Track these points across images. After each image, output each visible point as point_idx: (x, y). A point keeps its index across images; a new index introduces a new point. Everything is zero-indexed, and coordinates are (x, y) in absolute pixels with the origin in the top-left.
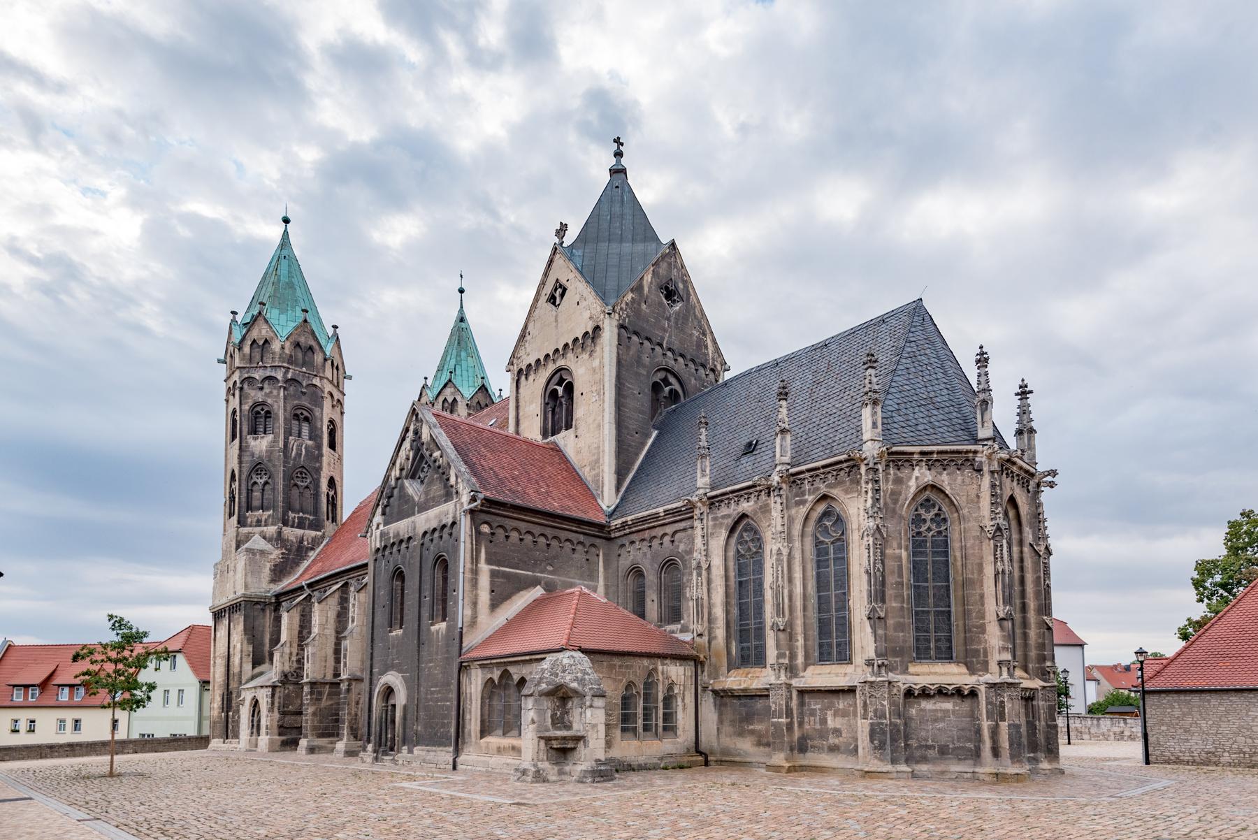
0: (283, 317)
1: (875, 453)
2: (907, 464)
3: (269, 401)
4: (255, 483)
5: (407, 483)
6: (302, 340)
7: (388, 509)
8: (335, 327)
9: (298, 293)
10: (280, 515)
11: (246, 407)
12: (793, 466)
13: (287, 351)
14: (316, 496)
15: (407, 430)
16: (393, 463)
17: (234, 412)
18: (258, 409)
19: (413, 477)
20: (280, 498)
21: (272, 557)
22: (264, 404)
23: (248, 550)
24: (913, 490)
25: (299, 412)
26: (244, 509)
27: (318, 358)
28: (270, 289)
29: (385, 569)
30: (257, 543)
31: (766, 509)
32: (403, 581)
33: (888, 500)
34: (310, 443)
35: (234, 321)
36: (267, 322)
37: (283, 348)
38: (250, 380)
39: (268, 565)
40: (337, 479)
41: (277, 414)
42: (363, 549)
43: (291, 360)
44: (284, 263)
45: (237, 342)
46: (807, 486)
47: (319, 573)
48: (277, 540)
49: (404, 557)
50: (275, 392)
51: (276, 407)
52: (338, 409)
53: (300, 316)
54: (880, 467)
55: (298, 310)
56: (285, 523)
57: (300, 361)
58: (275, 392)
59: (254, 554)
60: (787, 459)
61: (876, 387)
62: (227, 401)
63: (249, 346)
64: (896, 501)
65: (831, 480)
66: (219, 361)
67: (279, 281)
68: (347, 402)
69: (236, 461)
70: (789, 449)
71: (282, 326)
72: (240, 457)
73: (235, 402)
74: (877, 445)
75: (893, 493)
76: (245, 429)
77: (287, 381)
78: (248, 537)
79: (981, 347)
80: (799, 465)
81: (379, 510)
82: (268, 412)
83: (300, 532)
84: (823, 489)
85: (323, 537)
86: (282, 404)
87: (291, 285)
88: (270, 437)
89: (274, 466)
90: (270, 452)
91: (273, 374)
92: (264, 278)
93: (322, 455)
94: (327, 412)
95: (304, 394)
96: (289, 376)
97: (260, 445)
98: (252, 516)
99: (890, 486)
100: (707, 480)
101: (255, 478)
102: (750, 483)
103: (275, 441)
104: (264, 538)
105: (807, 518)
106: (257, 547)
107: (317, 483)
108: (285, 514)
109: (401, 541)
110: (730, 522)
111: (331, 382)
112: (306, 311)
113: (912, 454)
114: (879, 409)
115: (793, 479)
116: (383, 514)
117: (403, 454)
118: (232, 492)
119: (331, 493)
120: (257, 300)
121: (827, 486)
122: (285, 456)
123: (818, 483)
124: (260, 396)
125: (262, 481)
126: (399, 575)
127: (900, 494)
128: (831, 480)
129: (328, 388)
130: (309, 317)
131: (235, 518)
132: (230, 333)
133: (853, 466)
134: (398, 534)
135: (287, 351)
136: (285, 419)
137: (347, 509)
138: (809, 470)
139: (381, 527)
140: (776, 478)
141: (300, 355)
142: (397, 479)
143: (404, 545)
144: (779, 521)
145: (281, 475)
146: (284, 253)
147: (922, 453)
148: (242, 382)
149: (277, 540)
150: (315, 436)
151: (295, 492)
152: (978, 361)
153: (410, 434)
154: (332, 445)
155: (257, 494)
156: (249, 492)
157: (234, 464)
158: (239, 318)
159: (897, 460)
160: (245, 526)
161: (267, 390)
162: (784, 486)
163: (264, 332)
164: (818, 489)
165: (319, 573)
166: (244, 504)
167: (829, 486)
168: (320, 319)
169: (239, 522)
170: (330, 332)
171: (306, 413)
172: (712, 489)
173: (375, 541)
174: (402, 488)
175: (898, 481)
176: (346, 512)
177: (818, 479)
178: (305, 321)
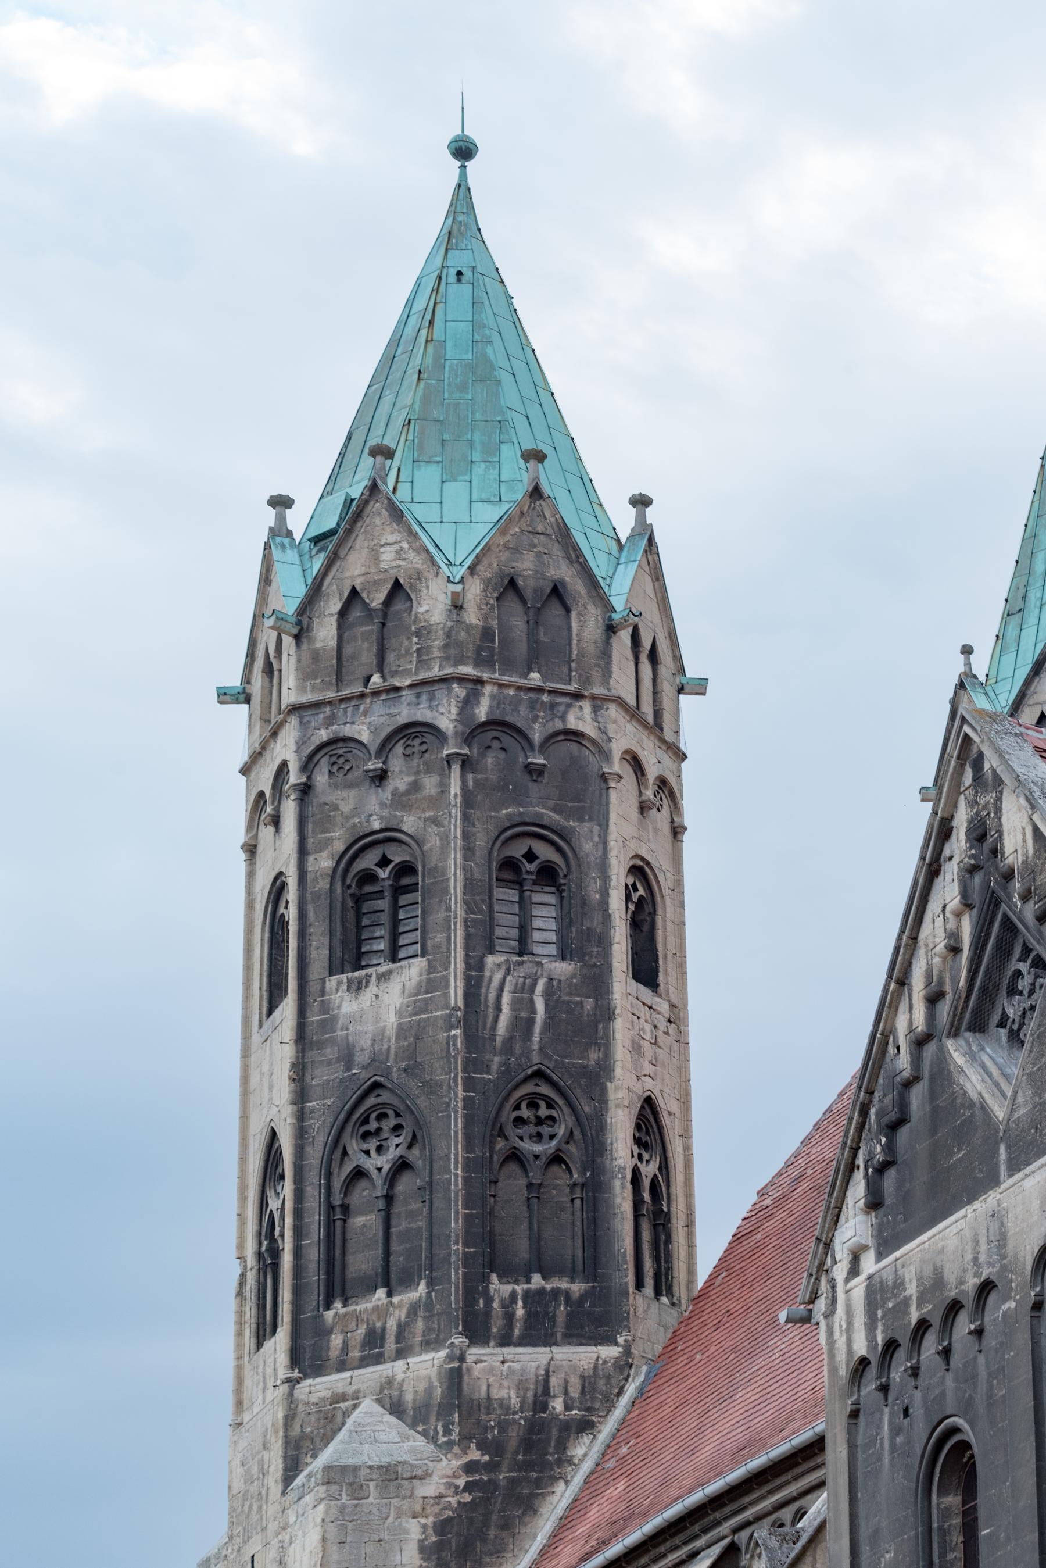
0: (456, 490)
3: (410, 823)
4: (359, 1174)
5: (956, 1052)
6: (525, 566)
7: (890, 1177)
8: (641, 502)
9: (510, 395)
10: (455, 1297)
11: (323, 862)
13: (472, 616)
14: (593, 1190)
15: (941, 831)
16: (899, 977)
17: (278, 888)
18: (368, 861)
19: (978, 1026)
20: (456, 1225)
21: (429, 1489)
22: (390, 836)
23: (334, 1475)
25: (517, 851)
26: (313, 1298)
27: (585, 626)
28: (410, 396)
29: (896, 1445)
30: (373, 1437)
32: (969, 1489)
34: (563, 969)
35: (279, 532)
36: (397, 514)
37: (457, 606)
38: (336, 750)
39: (414, 1530)
40: (667, 1104)
41: (438, 873)
42: (789, 1384)
43: (488, 649)
44: (458, 295)
45: (290, 608)
47: (617, 1526)
48: (445, 1410)
49: (969, 1377)
50: (430, 784)
51: (433, 842)
52: (661, 818)
53: (516, 476)
55: (510, 455)
56: (476, 1330)
57: (521, 649)
58: (430, 784)
59: (357, 1491)
62: (251, 850)
63: (337, 627)
66: (225, 696)
67: (440, 360)
68: (694, 784)
69: (283, 1090)
71: (456, 521)
72: (300, 1071)
73: (281, 851)
76: (319, 954)
77: (475, 732)
78: (331, 1418)
81: (858, 1190)
82: (407, 869)
83: (531, 1359)
85: (624, 1365)
86: (455, 829)
87: (481, 372)
88: (413, 971)
89: (431, 1088)
90: (413, 1033)
91: (423, 714)
92: (389, 359)
93: (607, 1014)
94: (623, 834)
95: (534, 772)
96: (482, 712)
97: (378, 1007)
98: (345, 1321)
101: (358, 1154)
103: (433, 984)
104: (396, 1409)
106: (369, 1455)
107: (592, 1136)
108: (474, 1288)
109: (954, 1307)
111: (634, 713)
112: (539, 457)
116: (874, 1203)
117: (934, 933)
118: (268, 1231)
119: (649, 1170)
120: (369, 445)
122: (472, 1039)
124: (371, 809)
125: (385, 1161)
126: (951, 1462)
129: (625, 736)
130: (550, 479)
131: (280, 1342)
132: (266, 579)
134: (939, 1281)
135: (472, 616)
136: (469, 885)
137: (711, 1226)
139: (869, 1264)
141: (518, 624)
142: (920, 1042)
143: (964, 1324)
145: (457, 1124)
146: (459, 260)
148: (308, 765)
149: (445, 1410)
150: (581, 941)
151: (513, 1185)
153: (958, 845)
154: (646, 971)
155: (365, 1222)
156: (337, 1215)
157: (277, 1107)
158: (298, 521)
160: (318, 1370)
161: (399, 781)
163: (388, 556)
165: (617, 1526)
166: (314, 1276)
168: (586, 482)
169: (296, 1358)
170: (624, 521)
171: (545, 852)
173: (848, 1330)
174: (943, 1075)
176: (709, 1236)
178: (536, 492)
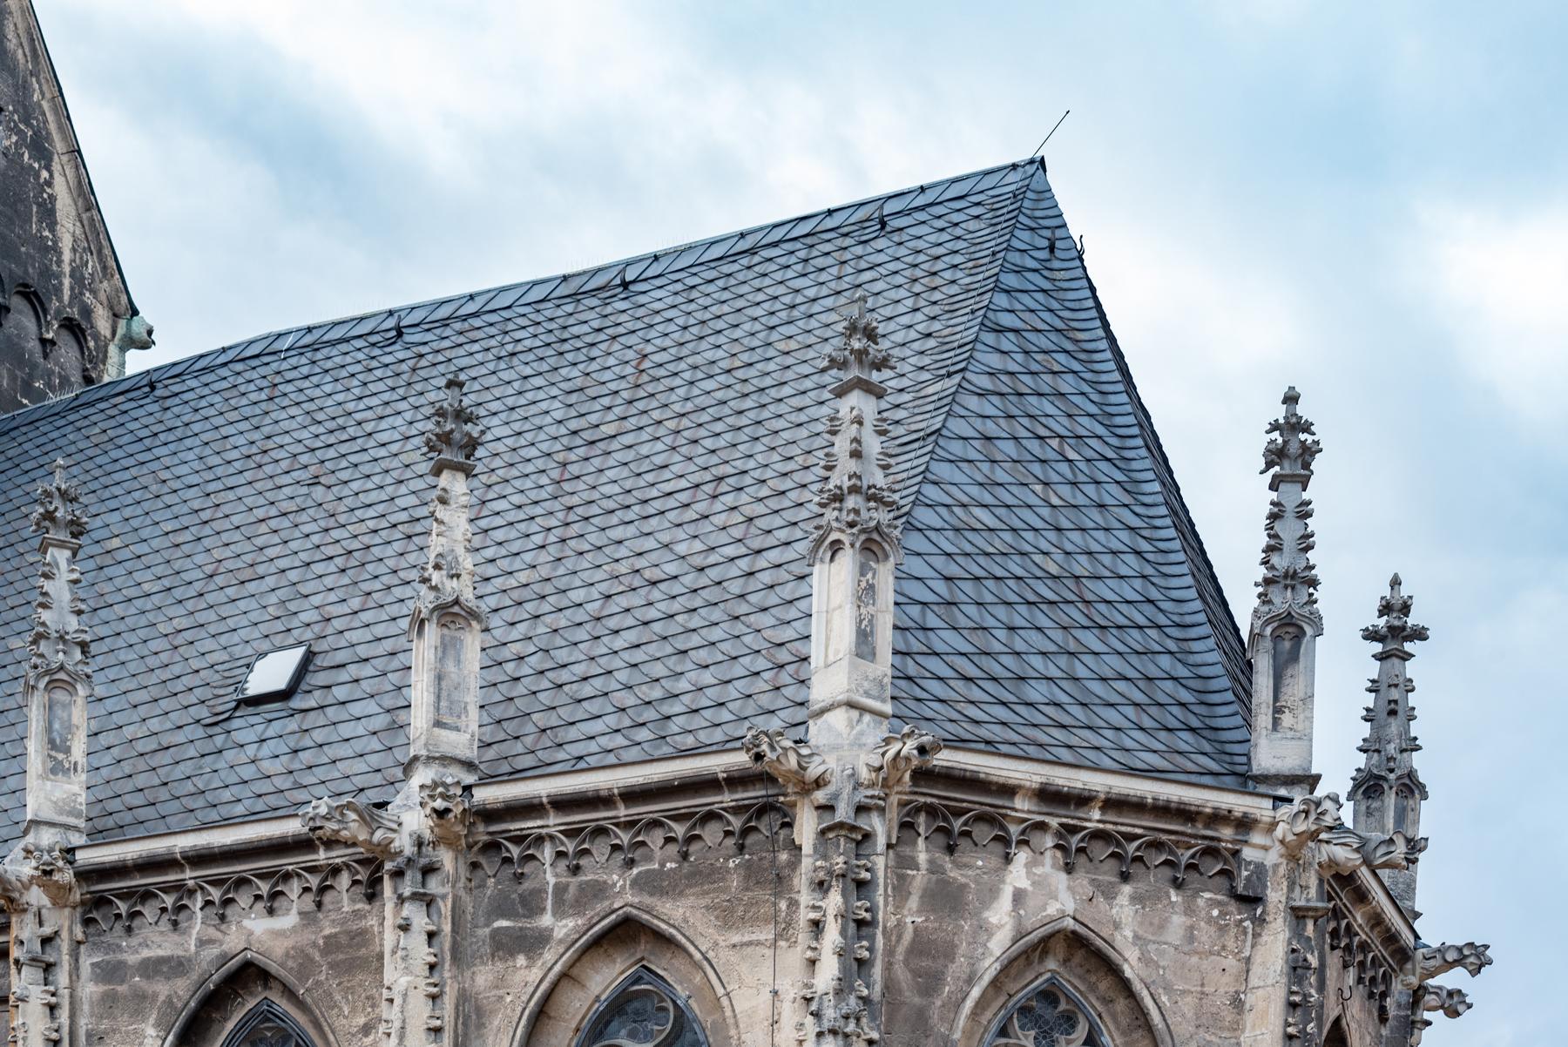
1: (864, 761)
2: (983, 833)
12: (489, 779)
24: (999, 944)
31: (355, 957)
33: (901, 974)
46: (550, 875)
54: (880, 828)
60: (460, 742)
61: (879, 479)
64: (930, 983)
65: (660, 857)
70: (472, 697)
74: (873, 732)
75: (922, 946)
79: (1291, 399)
80: (516, 775)
84: (623, 893)
99: (912, 916)
100: (74, 789)
102: (292, 827)
105: (541, 1015)
110: (181, 992)
113: (1009, 791)
114: (885, 577)
115: (490, 836)
121: (636, 883)
123: (601, 867)
127: (949, 953)
128: (660, 857)
133: (763, 810)
138: (562, 804)
140: (410, 820)
144: (420, 1012)
147: (1049, 796)
152: (1275, 455)
159: (948, 808)
162: (446, 858)
164: (599, 890)
167: (651, 884)
172: (98, 836)
175: (947, 899)
177: (600, 849)
